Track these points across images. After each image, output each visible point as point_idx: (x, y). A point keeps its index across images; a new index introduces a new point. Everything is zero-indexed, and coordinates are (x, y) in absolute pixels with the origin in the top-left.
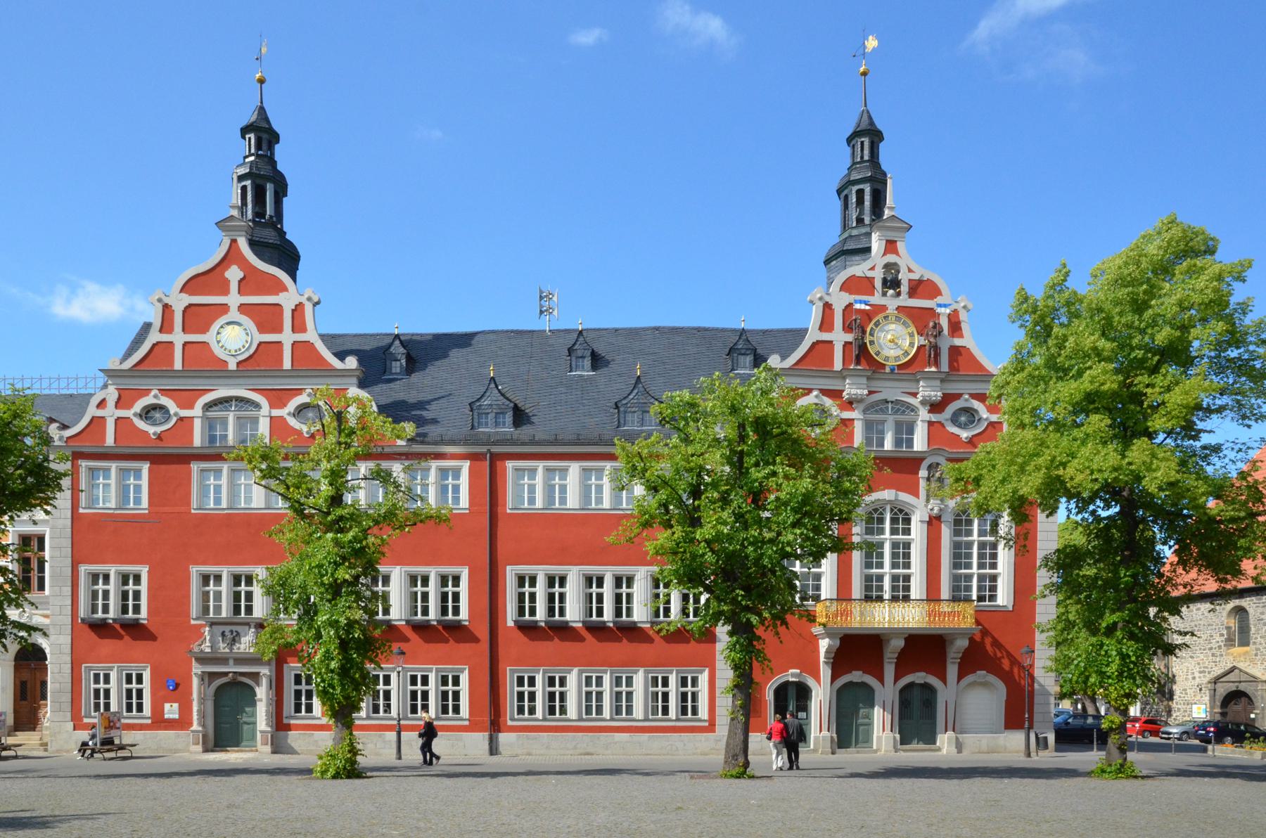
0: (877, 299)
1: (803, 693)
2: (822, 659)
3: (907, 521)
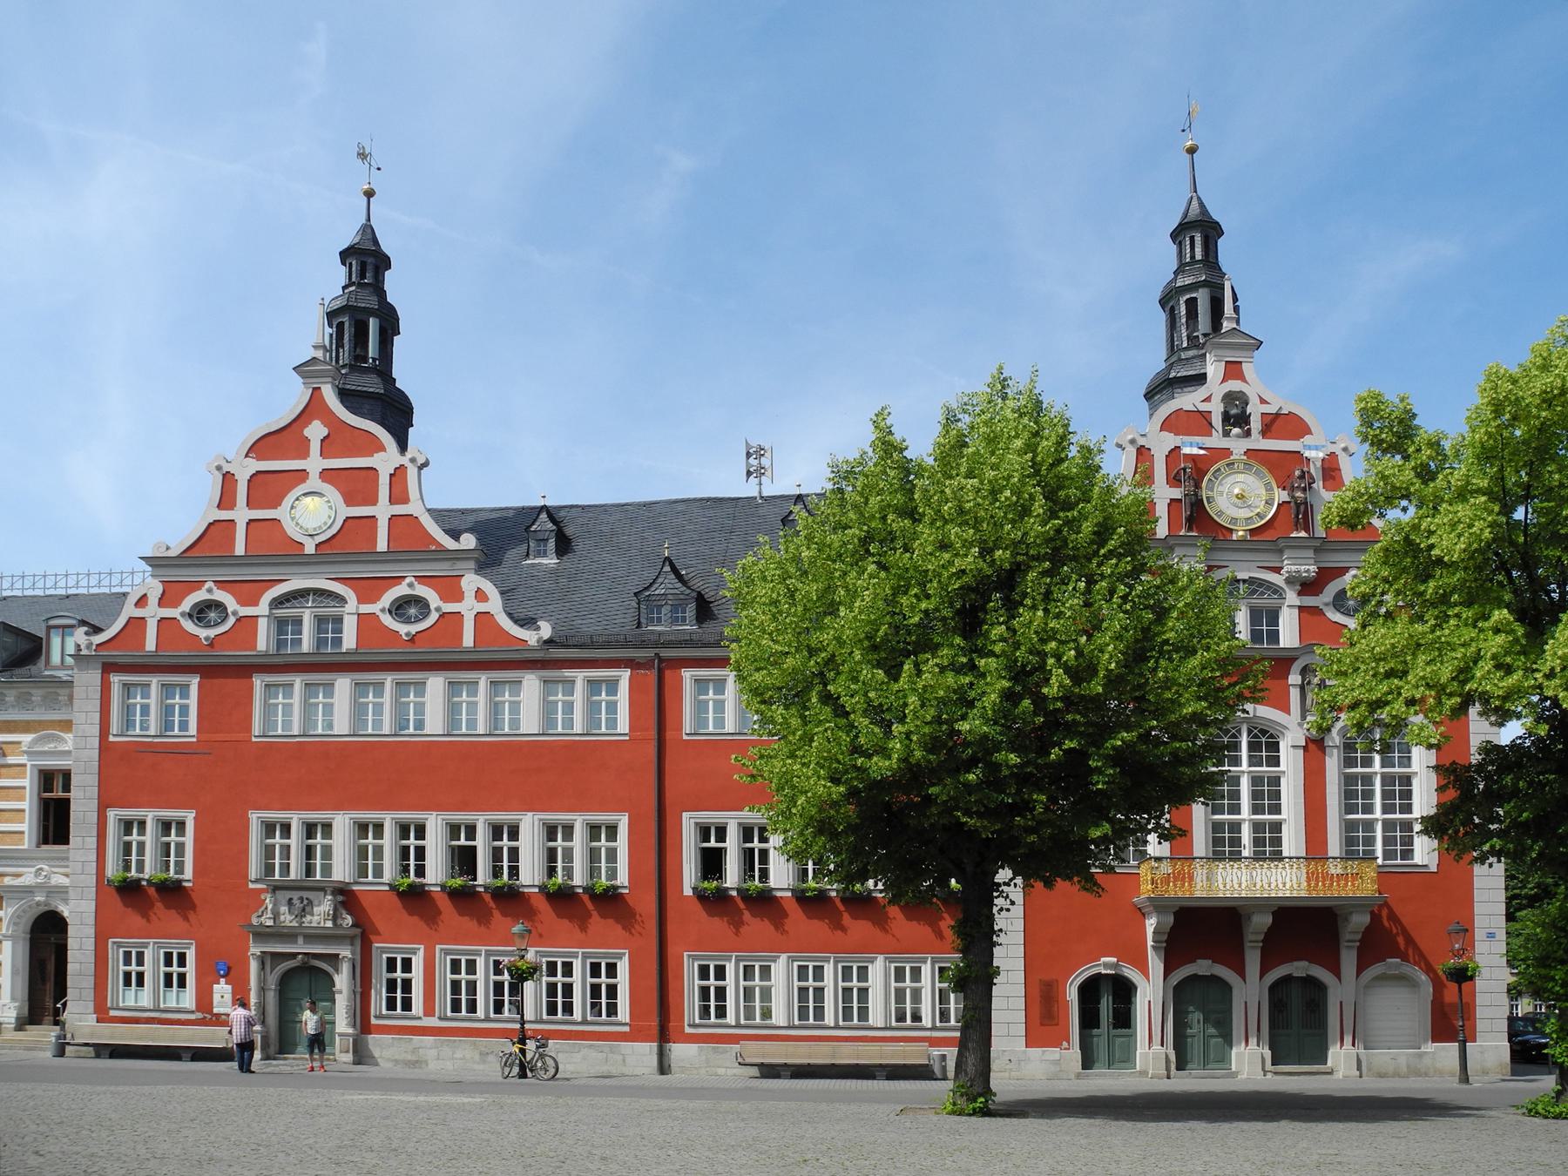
0: (1216, 440)
1: (1123, 991)
2: (1150, 943)
3: (1274, 746)
